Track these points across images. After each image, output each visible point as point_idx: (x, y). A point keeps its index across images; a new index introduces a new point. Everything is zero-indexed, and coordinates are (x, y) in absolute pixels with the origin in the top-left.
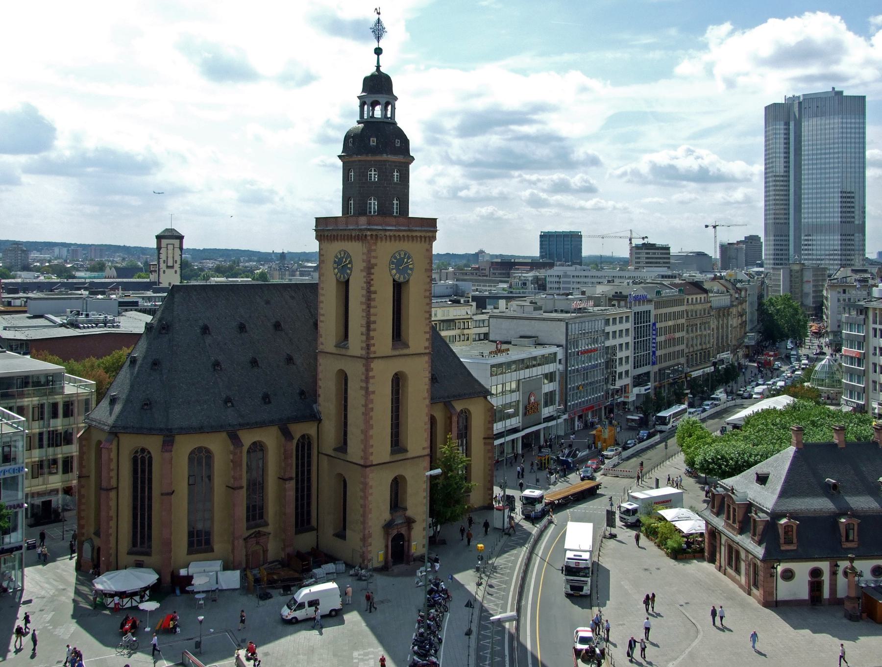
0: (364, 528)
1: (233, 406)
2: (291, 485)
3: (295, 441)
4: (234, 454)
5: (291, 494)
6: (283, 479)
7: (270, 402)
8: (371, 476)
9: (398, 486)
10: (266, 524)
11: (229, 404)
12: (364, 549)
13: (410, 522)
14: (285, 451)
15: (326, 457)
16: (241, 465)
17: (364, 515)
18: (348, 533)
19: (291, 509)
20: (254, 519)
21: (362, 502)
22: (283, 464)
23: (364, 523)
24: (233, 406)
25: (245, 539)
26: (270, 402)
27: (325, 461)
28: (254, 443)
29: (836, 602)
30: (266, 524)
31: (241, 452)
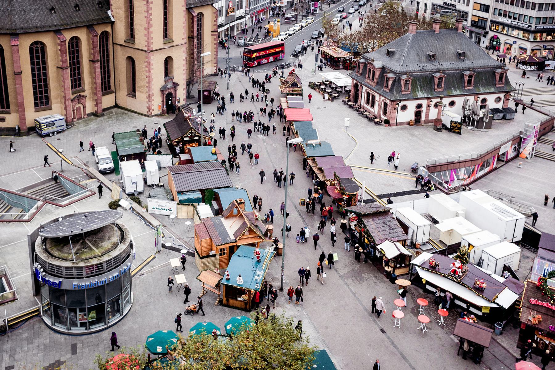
0: (149, 91)
1: (55, 12)
2: (98, 65)
3: (98, 36)
4: (61, 45)
5: (98, 70)
6: (92, 61)
7: (79, 10)
8: (152, 57)
9: (168, 61)
10: (84, 91)
11: (53, 12)
12: (150, 103)
13: (176, 85)
14: (93, 42)
15: (119, 46)
16: (66, 53)
17: (149, 82)
18: (138, 93)
19: (99, 81)
20: (76, 87)
21: (147, 74)
22: (92, 52)
23: (149, 87)
24: (55, 12)
25: (71, 100)
26: (79, 10)
27: (119, 49)
28: (72, 38)
29: (427, 122)
30: (84, 91)
31: (65, 44)
